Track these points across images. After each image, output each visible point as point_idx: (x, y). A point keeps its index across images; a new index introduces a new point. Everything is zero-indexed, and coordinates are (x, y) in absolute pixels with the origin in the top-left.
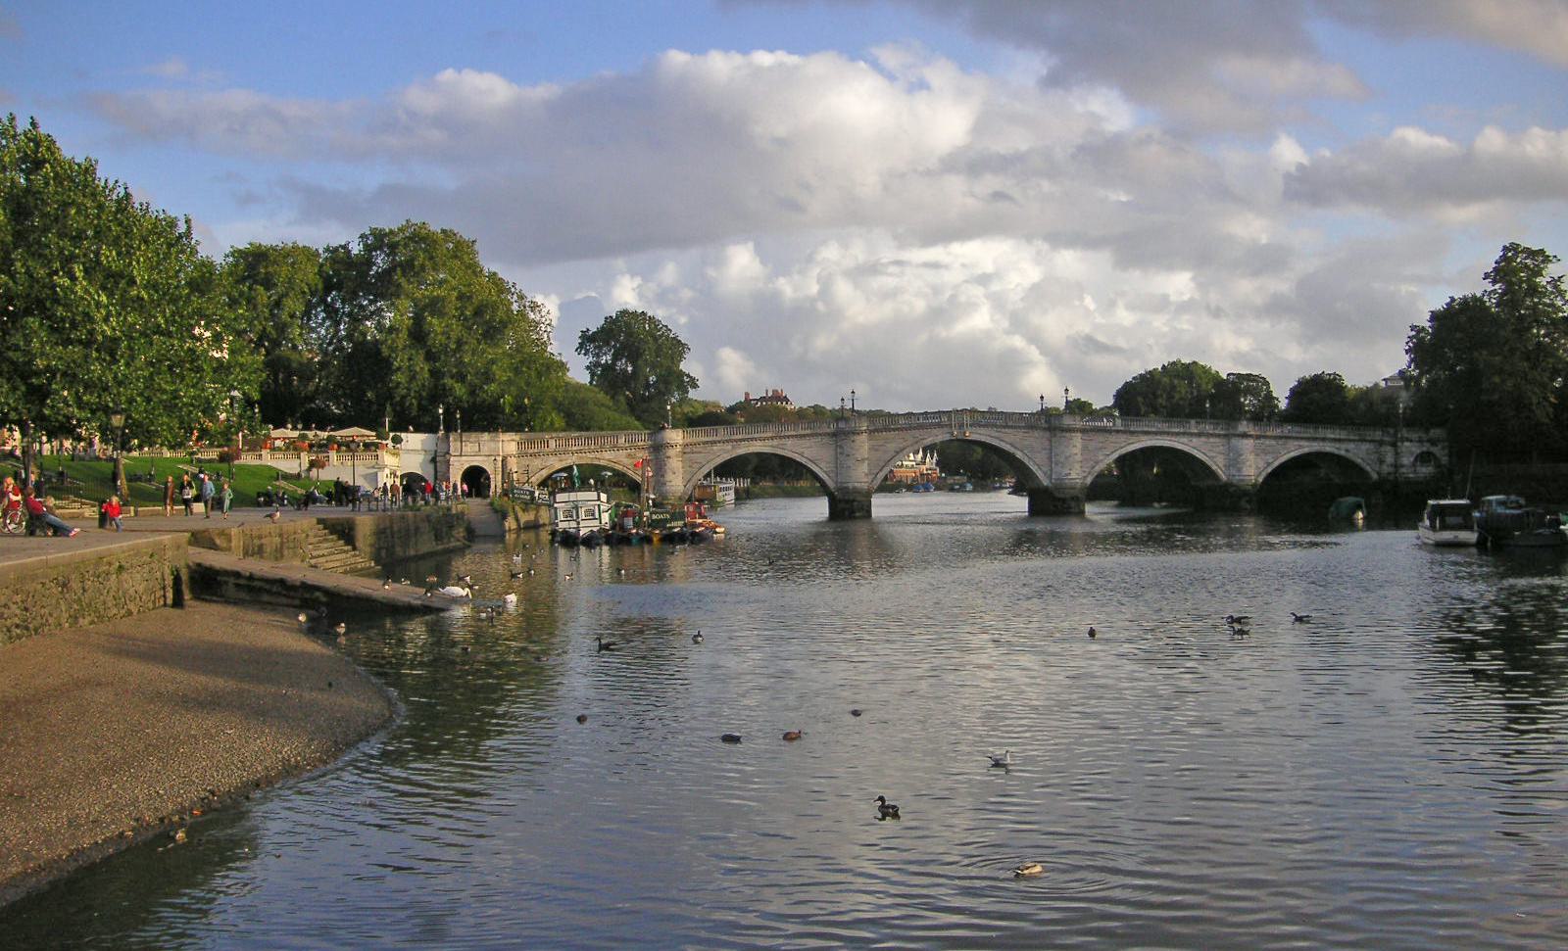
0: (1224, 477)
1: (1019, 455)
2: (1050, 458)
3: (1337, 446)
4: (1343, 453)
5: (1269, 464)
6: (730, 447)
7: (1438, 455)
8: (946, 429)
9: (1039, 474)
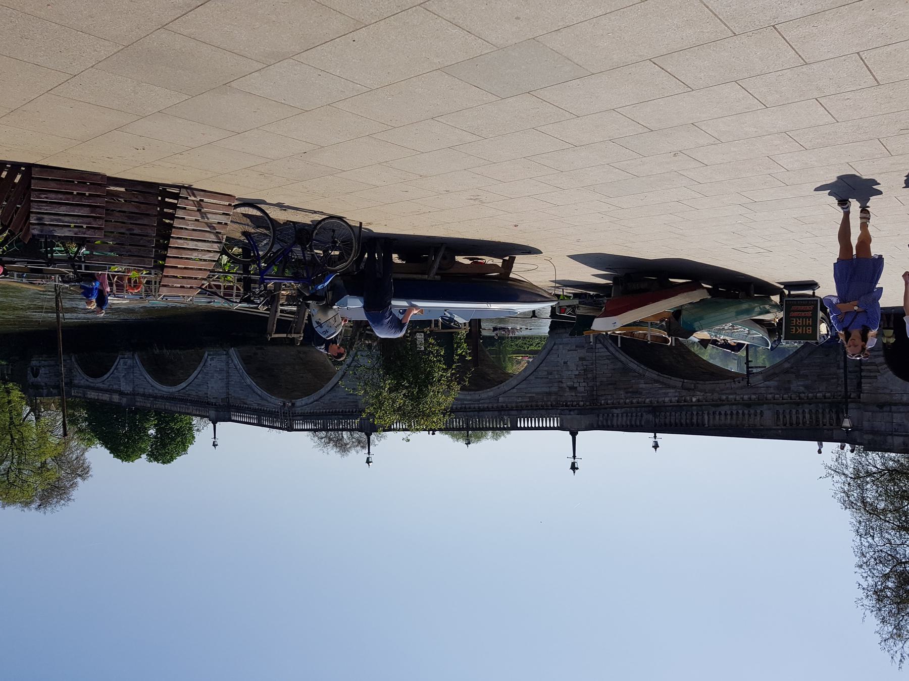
0: (136, 357)
1: (249, 380)
2: (228, 377)
3: (88, 383)
4: (86, 377)
5: (116, 368)
6: (501, 399)
7: (31, 374)
8: (298, 410)
9: (236, 361)
